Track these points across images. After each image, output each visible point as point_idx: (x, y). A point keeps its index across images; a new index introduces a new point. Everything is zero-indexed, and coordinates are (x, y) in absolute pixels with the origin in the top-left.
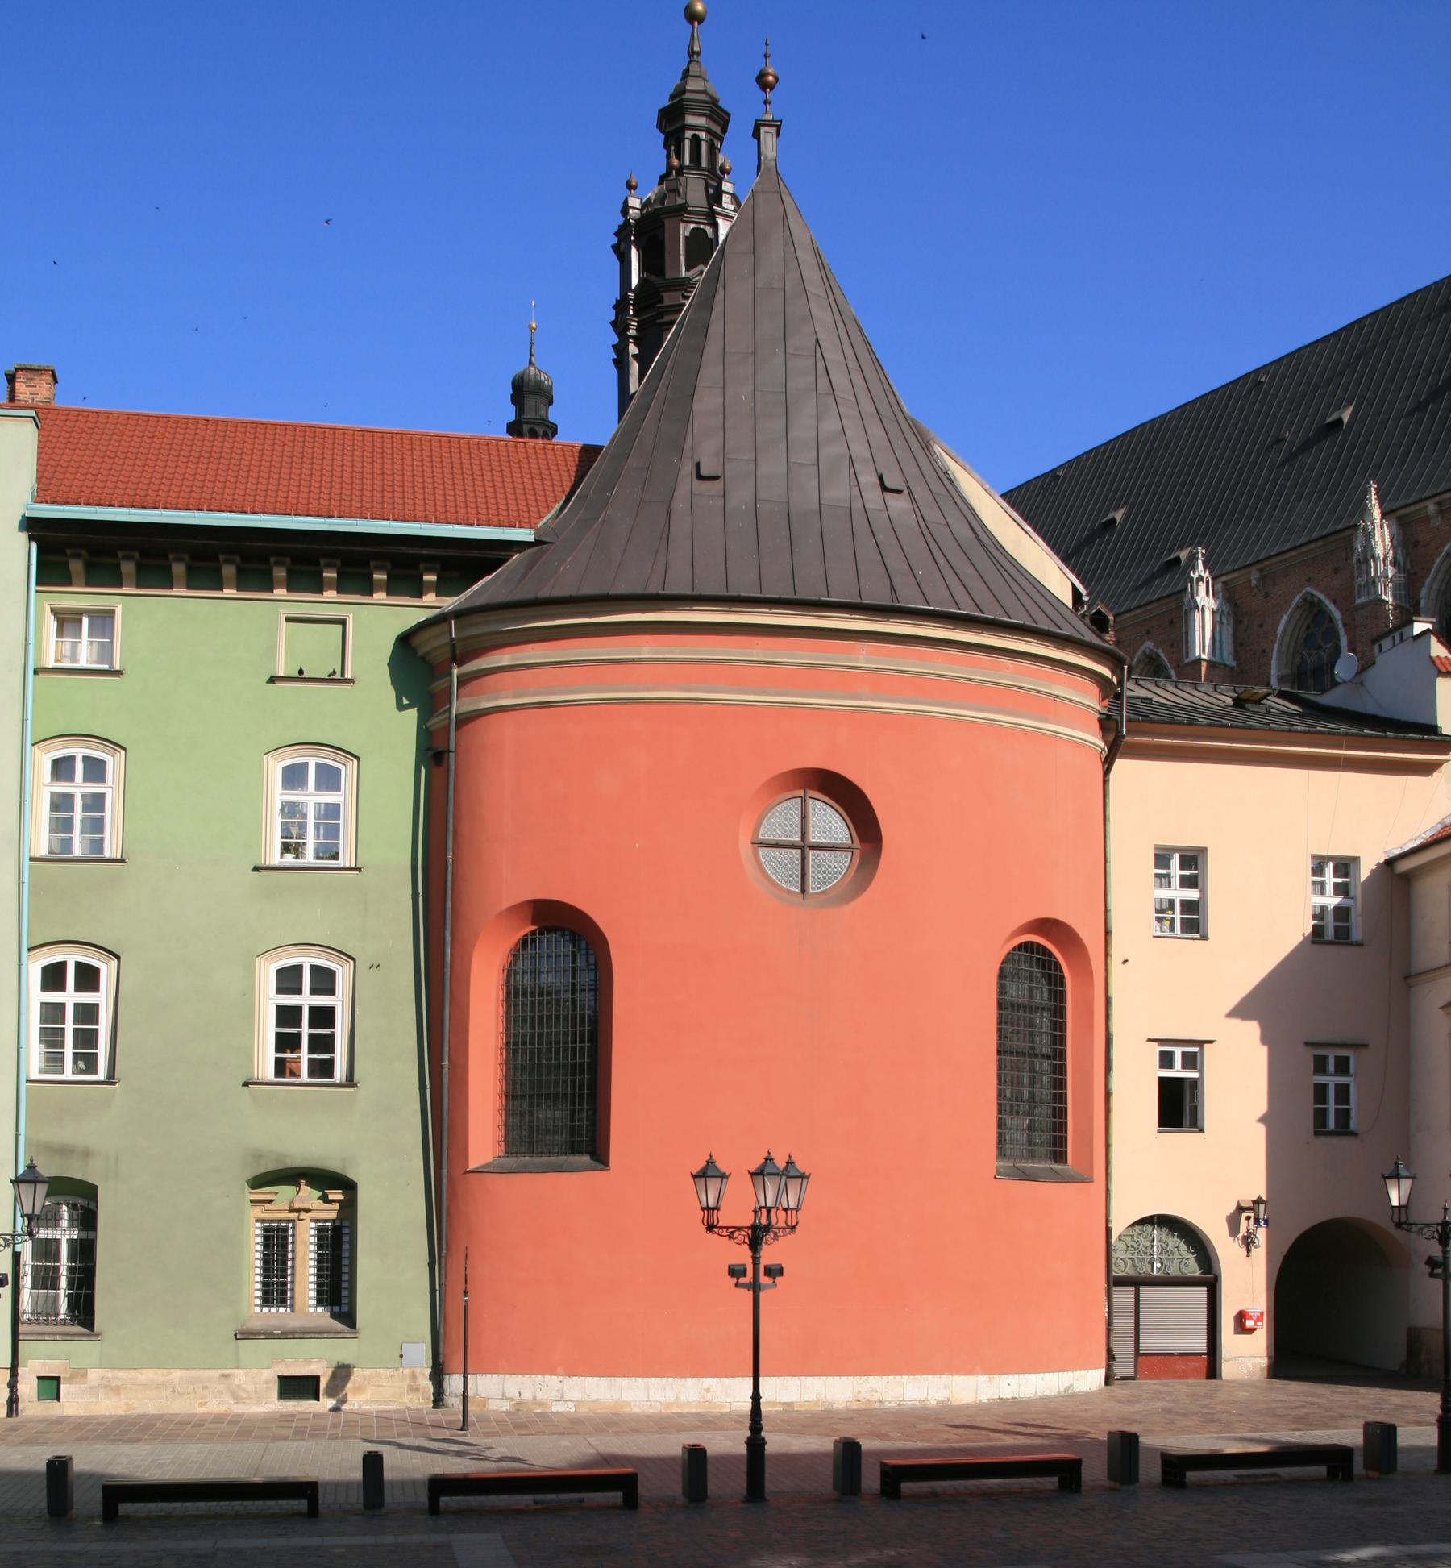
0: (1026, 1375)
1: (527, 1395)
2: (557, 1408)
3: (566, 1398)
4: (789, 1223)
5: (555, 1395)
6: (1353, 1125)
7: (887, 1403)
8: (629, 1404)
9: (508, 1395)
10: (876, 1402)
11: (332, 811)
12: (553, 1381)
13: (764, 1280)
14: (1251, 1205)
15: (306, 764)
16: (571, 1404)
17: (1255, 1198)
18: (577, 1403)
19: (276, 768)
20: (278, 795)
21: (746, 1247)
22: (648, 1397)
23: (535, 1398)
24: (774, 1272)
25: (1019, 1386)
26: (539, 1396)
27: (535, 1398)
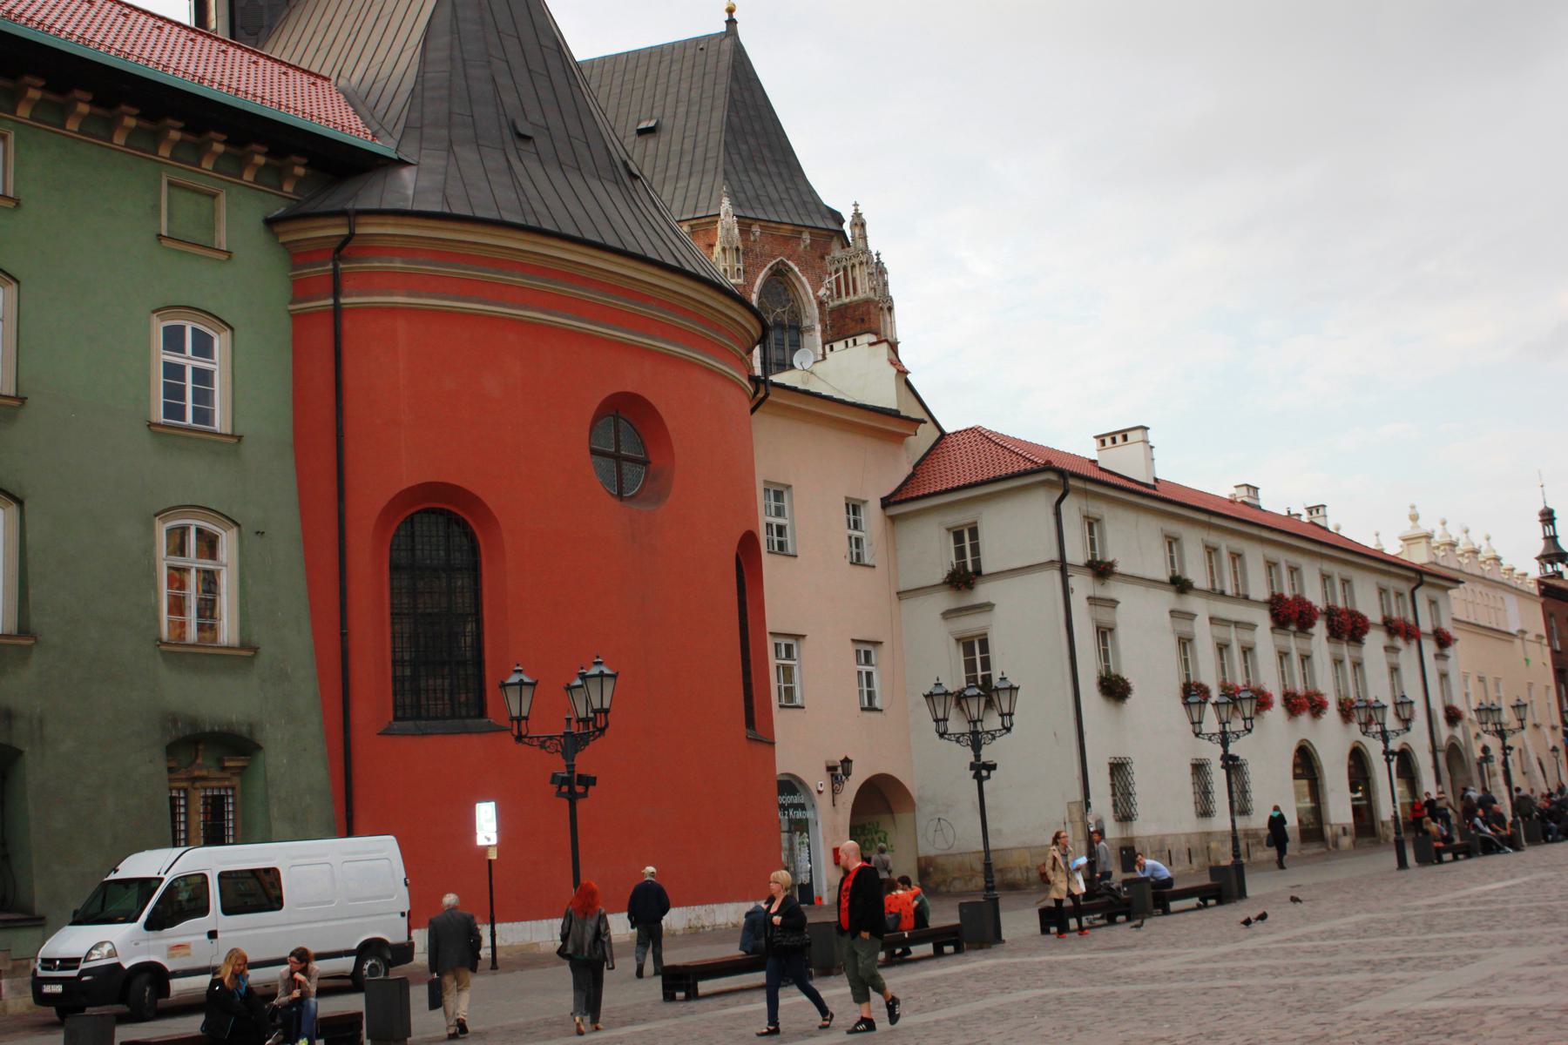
6: (877, 703)
8: (537, 944)
15: (182, 328)
17: (842, 758)
19: (158, 327)
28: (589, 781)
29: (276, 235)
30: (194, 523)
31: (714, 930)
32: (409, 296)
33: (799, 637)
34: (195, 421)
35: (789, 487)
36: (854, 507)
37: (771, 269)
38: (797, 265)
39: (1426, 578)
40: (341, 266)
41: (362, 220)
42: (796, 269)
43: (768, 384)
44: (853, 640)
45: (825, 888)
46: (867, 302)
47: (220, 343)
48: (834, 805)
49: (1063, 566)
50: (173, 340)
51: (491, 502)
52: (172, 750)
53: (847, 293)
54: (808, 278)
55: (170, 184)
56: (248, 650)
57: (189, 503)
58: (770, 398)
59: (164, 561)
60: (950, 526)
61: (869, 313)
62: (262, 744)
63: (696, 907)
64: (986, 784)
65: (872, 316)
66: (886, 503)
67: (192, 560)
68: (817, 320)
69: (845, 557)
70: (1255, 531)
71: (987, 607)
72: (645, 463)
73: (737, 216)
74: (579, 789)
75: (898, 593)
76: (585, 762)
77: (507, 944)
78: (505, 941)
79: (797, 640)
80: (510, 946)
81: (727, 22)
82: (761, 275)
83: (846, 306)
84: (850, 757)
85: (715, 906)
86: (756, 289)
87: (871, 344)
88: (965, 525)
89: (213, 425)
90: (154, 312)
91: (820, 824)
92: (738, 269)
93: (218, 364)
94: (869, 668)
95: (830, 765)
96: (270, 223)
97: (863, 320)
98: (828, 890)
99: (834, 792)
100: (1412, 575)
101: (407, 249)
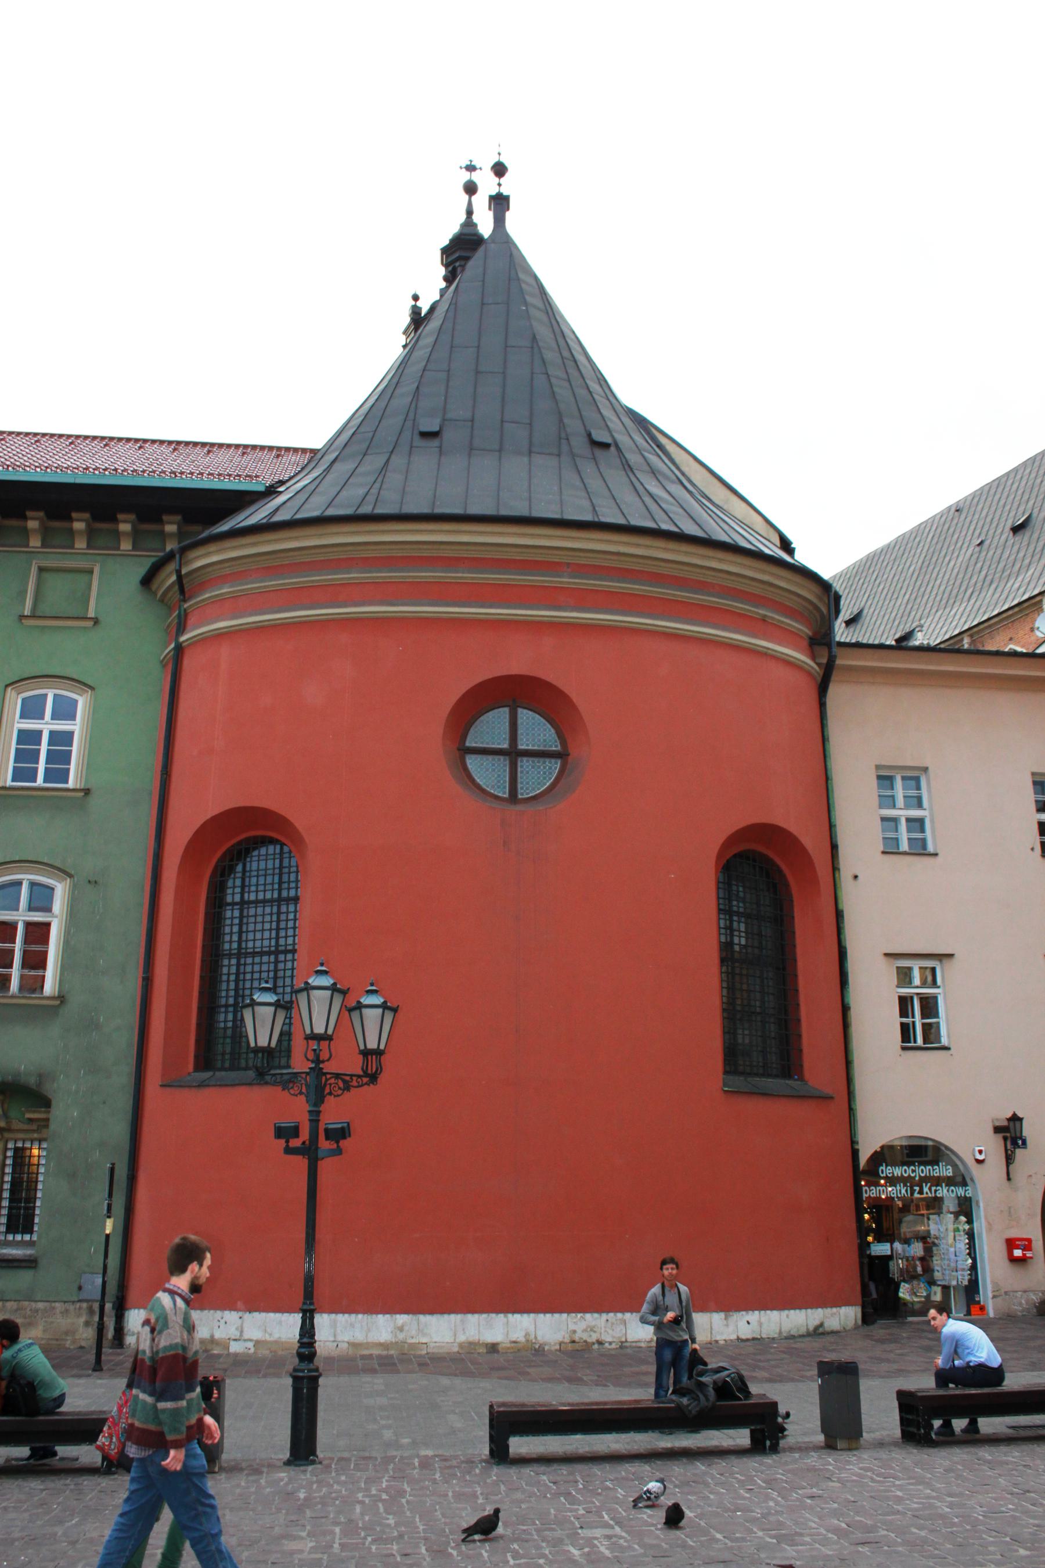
0: (768, 1312)
2: (235, 1348)
3: (246, 1336)
4: (369, 1072)
5: (233, 1332)
7: (607, 1345)
10: (594, 1344)
11: (57, 738)
12: (231, 1316)
13: (325, 1145)
14: (1005, 1123)
16: (250, 1345)
17: (1009, 1115)
18: (257, 1343)
21: (303, 1098)
22: (335, 1336)
23: (212, 1336)
24: (340, 1134)
25: (760, 1324)
26: (218, 1335)
29: (155, 593)
31: (621, 1347)
32: (232, 619)
33: (941, 957)
34: (45, 781)
35: (925, 769)
40: (186, 606)
43: (834, 646)
45: (990, 1295)
48: (1009, 1179)
50: (32, 709)
51: (300, 822)
57: (17, 859)
58: (838, 662)
63: (588, 1316)
64: (327, 1168)
69: (1032, 849)
72: (561, 755)
77: (272, 1339)
78: (270, 1335)
79: (941, 961)
80: (276, 1342)
84: (1020, 1115)
91: (981, 1204)
93: (76, 727)
95: (997, 1124)
96: (147, 581)
98: (994, 1297)
99: (1009, 1159)
101: (236, 570)
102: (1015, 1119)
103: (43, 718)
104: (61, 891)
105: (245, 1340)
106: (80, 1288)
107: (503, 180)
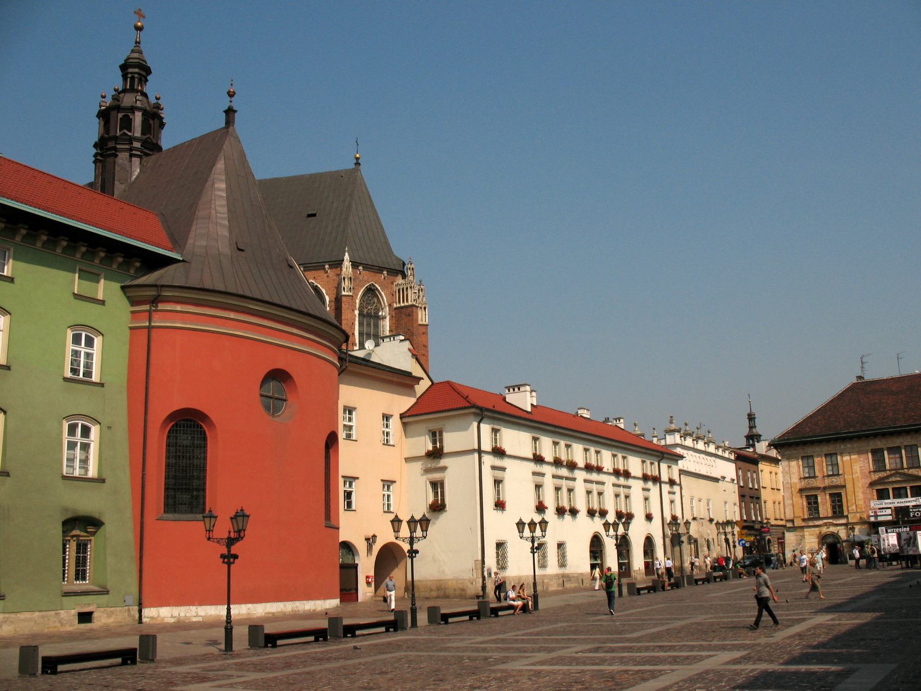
1: (182, 614)
2: (194, 619)
5: (194, 614)
9: (174, 615)
12: (193, 608)
15: (81, 334)
17: (372, 535)
19: (70, 334)
20: (70, 347)
23: (186, 616)
26: (188, 615)
27: (186, 616)
28: (236, 557)
30: (80, 423)
36: (387, 417)
37: (367, 287)
38: (379, 286)
39: (665, 456)
41: (164, 289)
42: (379, 288)
44: (382, 480)
46: (412, 306)
47: (98, 341)
49: (480, 451)
50: (77, 339)
52: (65, 523)
53: (403, 302)
54: (384, 293)
55: (79, 269)
56: (100, 480)
59: (66, 438)
60: (431, 428)
61: (413, 312)
62: (104, 522)
64: (414, 559)
65: (414, 313)
66: (402, 416)
67: (78, 438)
68: (388, 313)
70: (578, 435)
71: (444, 469)
73: (352, 262)
74: (232, 560)
75: (405, 459)
76: (235, 549)
81: (355, 164)
82: (362, 291)
83: (402, 308)
84: (376, 535)
85: (305, 602)
86: (359, 297)
87: (401, 341)
88: (437, 429)
89: (91, 378)
90: (69, 327)
92: (350, 288)
94: (389, 493)
97: (409, 315)
100: (659, 454)
102: (374, 536)
103: (81, 345)
104: (95, 431)
105: (199, 616)
106: (125, 601)
107: (233, 99)
